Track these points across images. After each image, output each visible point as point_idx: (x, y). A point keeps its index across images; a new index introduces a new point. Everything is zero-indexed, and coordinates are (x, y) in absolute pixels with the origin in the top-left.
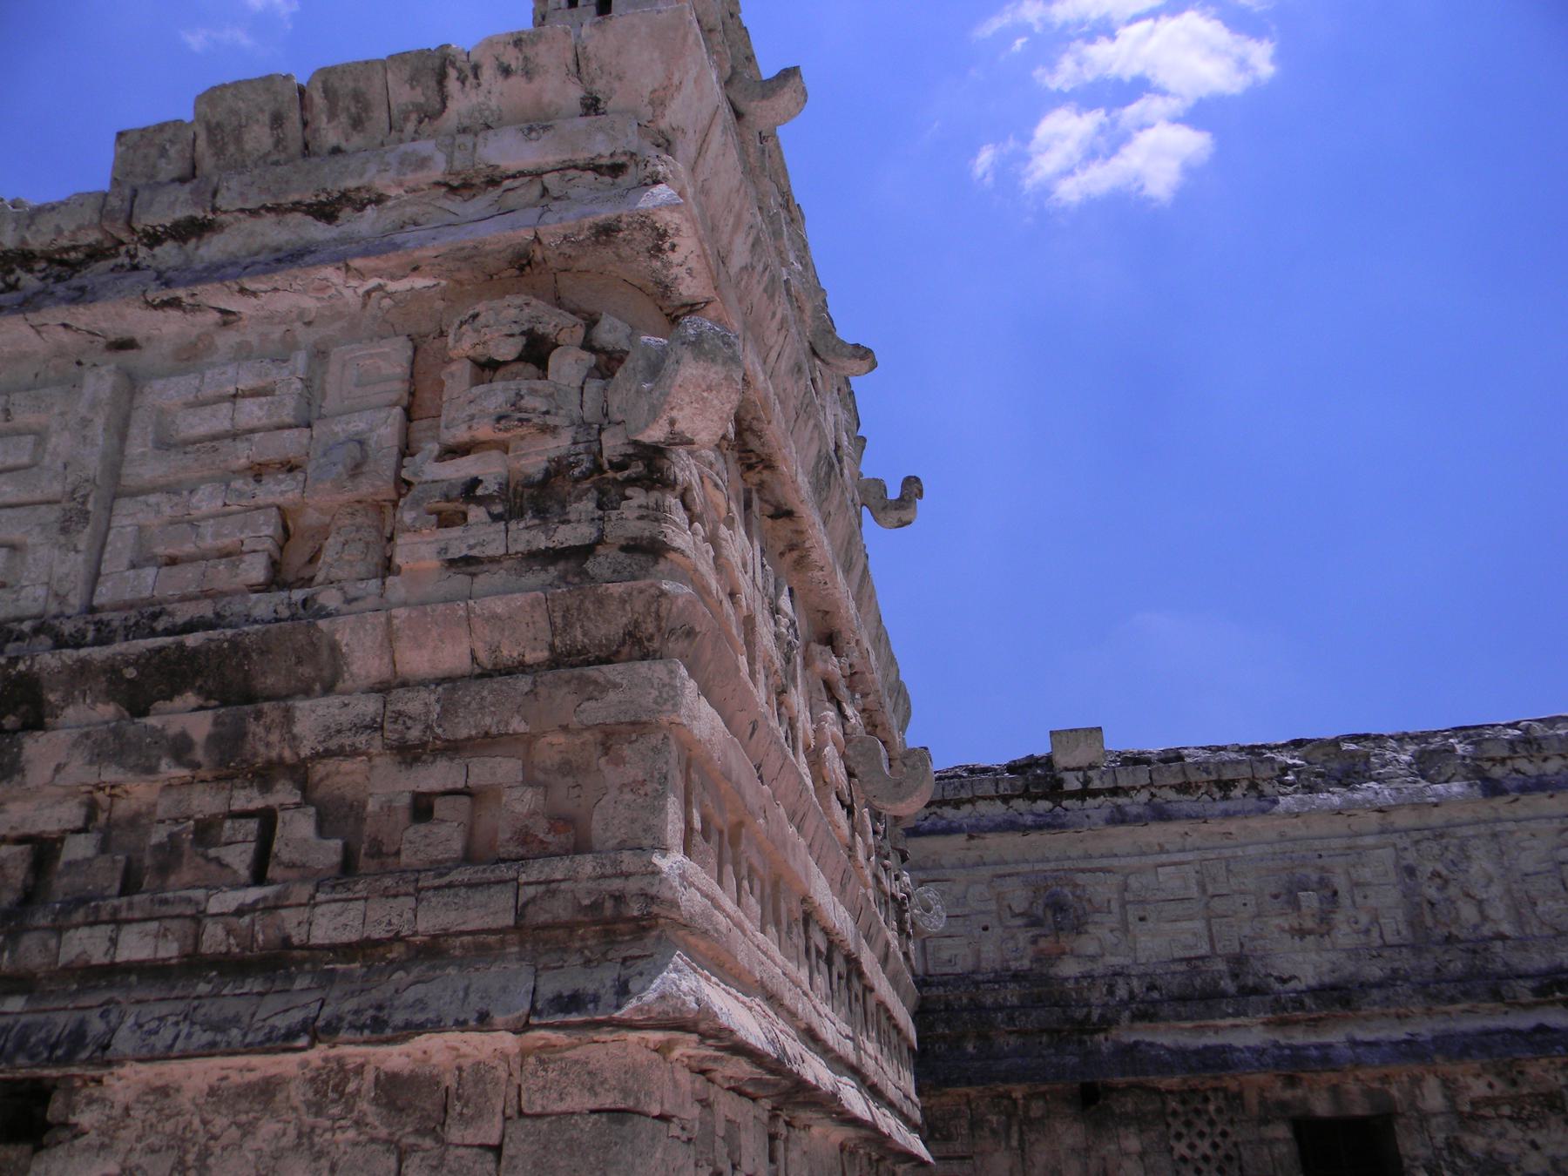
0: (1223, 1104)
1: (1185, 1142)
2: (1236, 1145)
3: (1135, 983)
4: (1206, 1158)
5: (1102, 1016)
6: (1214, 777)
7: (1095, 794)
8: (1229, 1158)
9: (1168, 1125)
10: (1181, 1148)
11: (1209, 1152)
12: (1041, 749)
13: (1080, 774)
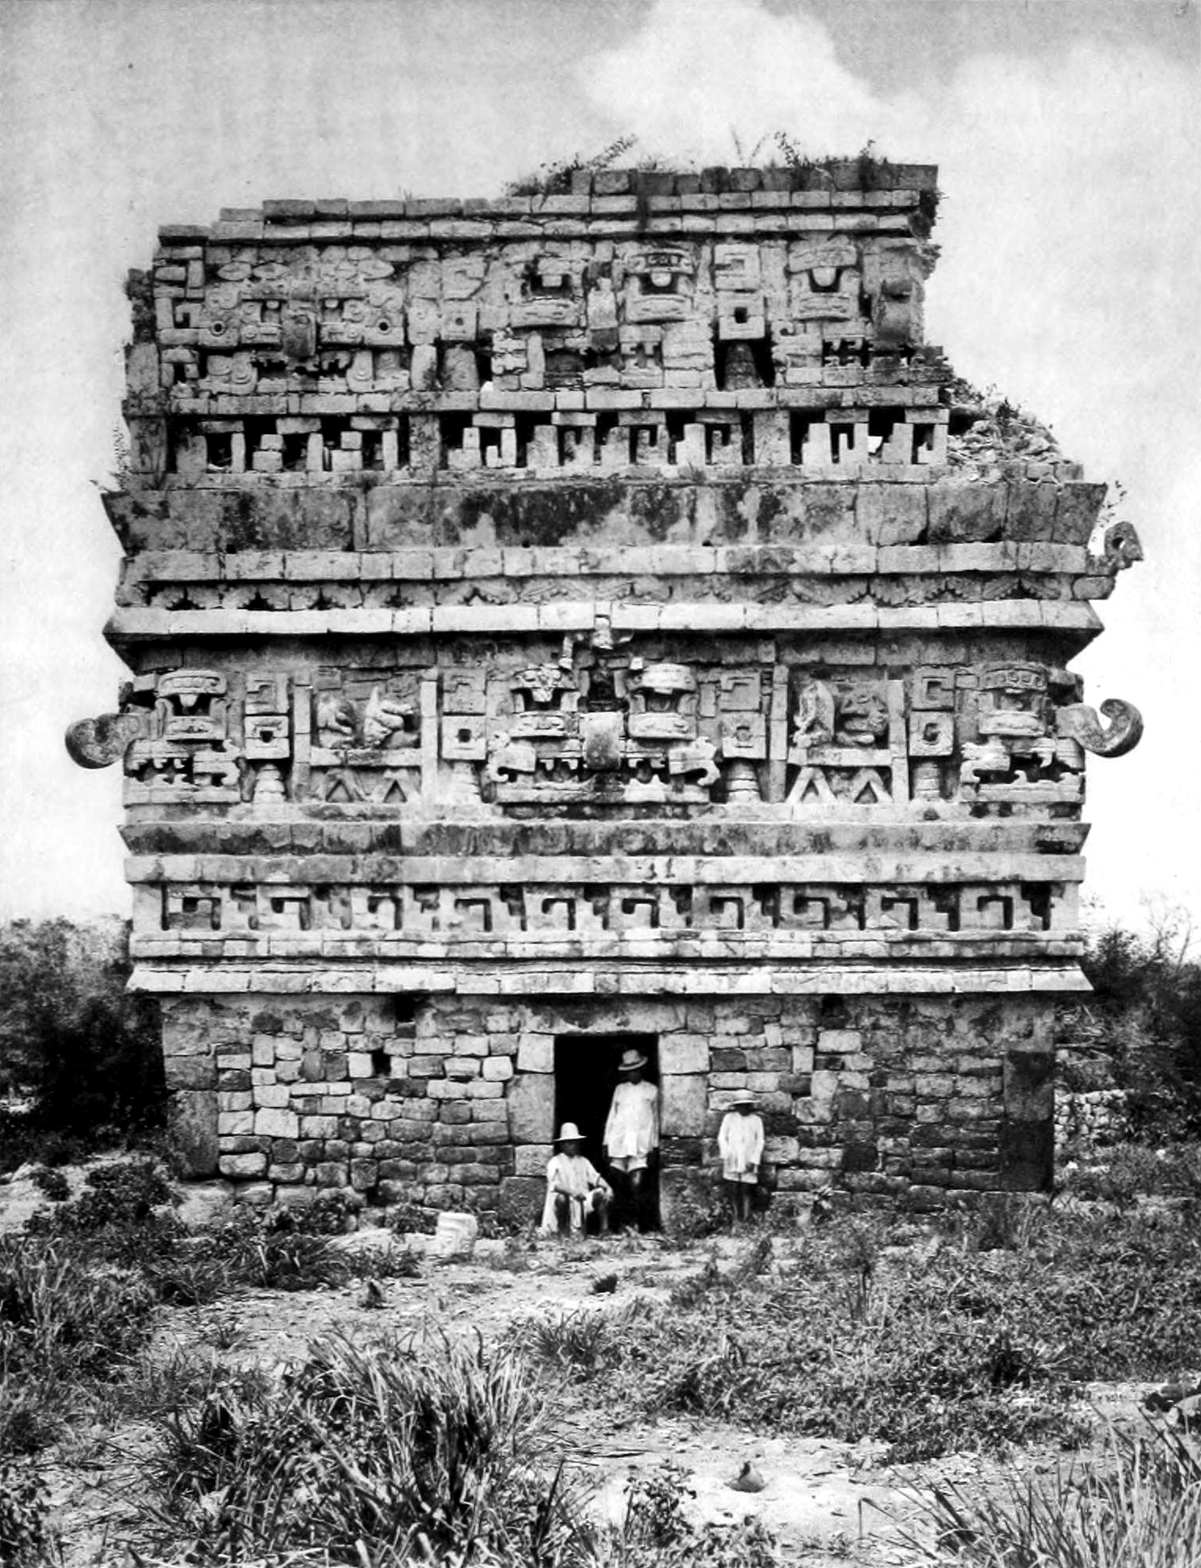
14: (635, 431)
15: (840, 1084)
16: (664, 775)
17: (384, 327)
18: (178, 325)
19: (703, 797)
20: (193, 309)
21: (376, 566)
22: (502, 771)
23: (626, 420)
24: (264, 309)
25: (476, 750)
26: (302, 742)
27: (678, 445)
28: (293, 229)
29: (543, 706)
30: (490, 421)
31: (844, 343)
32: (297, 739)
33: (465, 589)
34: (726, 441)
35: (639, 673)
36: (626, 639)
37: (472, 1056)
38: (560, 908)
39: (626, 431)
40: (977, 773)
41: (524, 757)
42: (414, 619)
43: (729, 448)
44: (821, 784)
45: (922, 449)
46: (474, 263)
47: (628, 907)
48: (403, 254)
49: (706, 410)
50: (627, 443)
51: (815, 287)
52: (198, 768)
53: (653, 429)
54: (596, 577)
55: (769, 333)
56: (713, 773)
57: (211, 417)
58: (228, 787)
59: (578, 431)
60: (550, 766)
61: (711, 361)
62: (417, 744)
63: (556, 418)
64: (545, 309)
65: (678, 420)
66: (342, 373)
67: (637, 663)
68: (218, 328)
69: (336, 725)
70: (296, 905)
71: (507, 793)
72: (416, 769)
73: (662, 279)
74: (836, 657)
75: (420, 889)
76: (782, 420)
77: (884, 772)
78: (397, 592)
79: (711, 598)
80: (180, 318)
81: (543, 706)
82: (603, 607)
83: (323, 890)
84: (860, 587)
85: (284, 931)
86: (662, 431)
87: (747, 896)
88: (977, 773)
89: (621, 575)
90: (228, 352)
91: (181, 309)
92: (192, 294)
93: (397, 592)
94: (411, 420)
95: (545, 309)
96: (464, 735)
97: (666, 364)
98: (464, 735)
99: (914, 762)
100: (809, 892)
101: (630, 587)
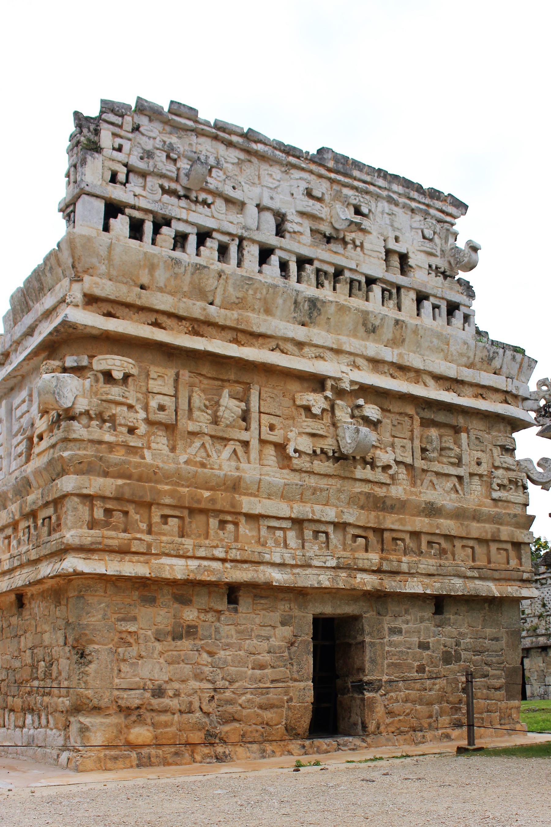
14: (352, 281)
16: (373, 465)
22: (296, 451)
23: (347, 274)
25: (277, 437)
27: (370, 293)
29: (314, 416)
30: (285, 256)
33: (273, 344)
34: (390, 298)
35: (359, 407)
36: (356, 387)
39: (348, 280)
43: (391, 302)
50: (348, 286)
54: (338, 352)
55: (408, 253)
56: (395, 467)
58: (139, 437)
59: (326, 273)
60: (318, 451)
61: (384, 257)
62: (246, 429)
63: (317, 264)
65: (371, 281)
67: (361, 402)
69: (204, 408)
70: (176, 520)
72: (246, 444)
74: (441, 417)
76: (413, 295)
77: (460, 478)
78: (242, 335)
79: (388, 374)
81: (314, 416)
83: (192, 511)
87: (407, 537)
89: (350, 354)
96: (272, 428)
97: (366, 251)
98: (272, 428)
99: (472, 475)
101: (355, 359)
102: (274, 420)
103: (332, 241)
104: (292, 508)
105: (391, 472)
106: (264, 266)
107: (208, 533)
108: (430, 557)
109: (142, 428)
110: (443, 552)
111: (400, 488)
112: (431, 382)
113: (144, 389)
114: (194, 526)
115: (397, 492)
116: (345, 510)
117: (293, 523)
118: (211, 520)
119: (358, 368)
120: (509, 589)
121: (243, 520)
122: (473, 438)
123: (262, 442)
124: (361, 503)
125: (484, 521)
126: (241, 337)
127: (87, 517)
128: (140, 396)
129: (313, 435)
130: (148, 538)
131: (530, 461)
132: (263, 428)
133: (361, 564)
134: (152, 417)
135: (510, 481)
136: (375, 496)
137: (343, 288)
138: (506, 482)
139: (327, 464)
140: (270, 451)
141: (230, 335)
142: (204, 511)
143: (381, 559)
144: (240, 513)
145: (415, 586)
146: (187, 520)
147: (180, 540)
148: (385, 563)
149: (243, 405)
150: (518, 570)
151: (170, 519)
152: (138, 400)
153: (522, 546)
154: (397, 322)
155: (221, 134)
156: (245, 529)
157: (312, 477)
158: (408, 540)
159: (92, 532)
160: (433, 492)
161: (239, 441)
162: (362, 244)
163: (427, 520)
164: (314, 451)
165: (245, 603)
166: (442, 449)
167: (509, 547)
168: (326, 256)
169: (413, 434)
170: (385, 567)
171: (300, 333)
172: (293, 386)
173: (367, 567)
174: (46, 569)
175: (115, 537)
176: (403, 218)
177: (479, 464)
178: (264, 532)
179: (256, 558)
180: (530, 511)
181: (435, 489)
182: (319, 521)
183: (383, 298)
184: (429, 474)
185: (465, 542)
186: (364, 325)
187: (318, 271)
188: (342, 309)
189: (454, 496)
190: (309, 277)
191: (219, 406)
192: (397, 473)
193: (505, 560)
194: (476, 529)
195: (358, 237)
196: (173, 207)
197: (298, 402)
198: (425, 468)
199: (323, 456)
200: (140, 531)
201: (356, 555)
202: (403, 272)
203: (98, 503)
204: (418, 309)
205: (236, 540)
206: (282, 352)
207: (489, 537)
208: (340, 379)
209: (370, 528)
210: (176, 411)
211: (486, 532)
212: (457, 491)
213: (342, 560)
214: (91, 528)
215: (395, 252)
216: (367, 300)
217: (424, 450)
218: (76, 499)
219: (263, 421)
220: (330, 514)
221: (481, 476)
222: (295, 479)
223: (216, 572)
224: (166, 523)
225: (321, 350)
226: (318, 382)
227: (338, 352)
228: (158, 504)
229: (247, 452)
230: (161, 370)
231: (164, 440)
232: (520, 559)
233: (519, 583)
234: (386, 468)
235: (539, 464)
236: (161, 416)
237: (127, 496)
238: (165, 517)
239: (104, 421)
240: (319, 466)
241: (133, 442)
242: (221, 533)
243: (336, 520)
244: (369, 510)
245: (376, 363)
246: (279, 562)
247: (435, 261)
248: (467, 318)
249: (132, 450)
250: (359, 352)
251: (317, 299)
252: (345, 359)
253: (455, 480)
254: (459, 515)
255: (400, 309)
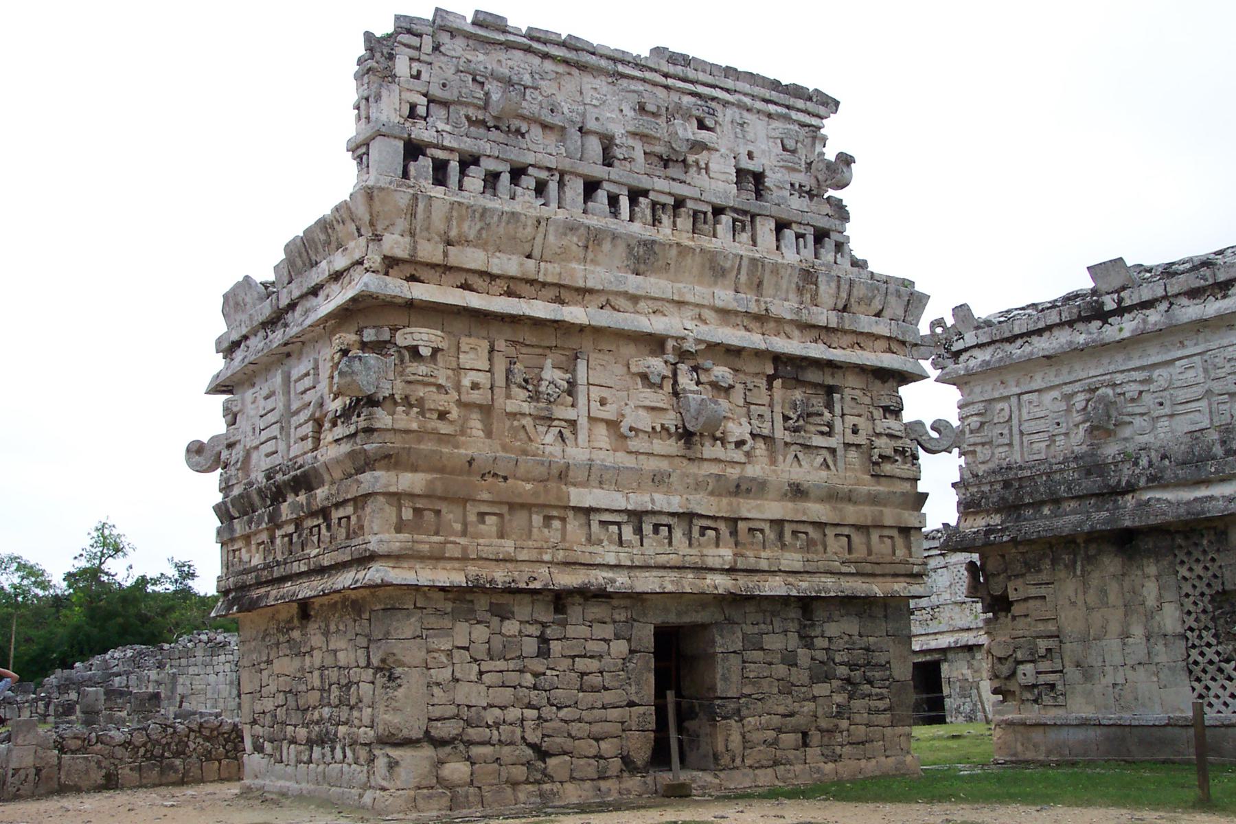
0: (1213, 538)
1: (1186, 566)
2: (1220, 567)
3: (1153, 454)
4: (1200, 577)
5: (1128, 482)
6: (1211, 281)
7: (1129, 309)
8: (1215, 576)
9: (1175, 556)
10: (1183, 571)
11: (1201, 574)
12: (1087, 284)
13: (1115, 296)
14: (695, 213)
15: (813, 659)
16: (724, 442)
17: (552, 111)
18: (412, 76)
19: (743, 460)
20: (425, 69)
21: (550, 272)
22: (631, 429)
24: (474, 80)
25: (609, 412)
26: (500, 393)
28: (489, 31)
31: (800, 186)
32: (496, 390)
33: (603, 300)
34: (743, 229)
36: (703, 347)
37: (604, 640)
38: (664, 531)
39: (691, 212)
40: (880, 456)
41: (645, 421)
42: (575, 314)
43: (744, 235)
44: (800, 455)
45: (839, 256)
46: (601, 83)
47: (703, 530)
48: (561, 69)
49: (735, 210)
51: (784, 149)
52: (429, 405)
53: (705, 213)
54: (680, 304)
56: (750, 442)
57: (436, 146)
58: (451, 422)
59: (664, 206)
60: (658, 429)
63: (652, 195)
64: (646, 125)
65: (718, 211)
66: (523, 135)
68: (444, 85)
70: (494, 518)
71: (634, 444)
72: (573, 423)
73: (709, 122)
75: (577, 510)
76: (773, 226)
77: (833, 451)
80: (415, 73)
81: (651, 385)
82: (689, 325)
83: (512, 507)
84: (815, 333)
85: (487, 539)
86: (710, 215)
87: (766, 527)
88: (880, 456)
90: (445, 104)
91: (416, 66)
92: (423, 57)
93: (562, 292)
94: (567, 178)
95: (646, 125)
96: (603, 402)
98: (603, 402)
99: (847, 445)
100: (801, 528)
102: (605, 393)
103: (671, 164)
104: (628, 498)
105: (746, 448)
106: (590, 204)
107: (530, 531)
108: (793, 548)
109: (455, 413)
110: (810, 544)
111: (758, 467)
112: (797, 333)
113: (454, 365)
114: (515, 524)
115: (753, 471)
116: (691, 497)
117: (629, 516)
118: (534, 517)
119: (705, 322)
120: (896, 587)
121: (571, 514)
122: (848, 398)
123: (591, 419)
124: (710, 488)
125: (863, 503)
126: (565, 295)
127: (394, 519)
128: (450, 372)
129: (653, 409)
130: (463, 541)
131: (920, 423)
132: (592, 403)
133: (710, 562)
134: (464, 398)
135: (896, 451)
136: (727, 479)
137: (684, 222)
138: (890, 452)
139: (668, 442)
140: (602, 430)
141: (552, 293)
142: (527, 507)
143: (735, 555)
144: (566, 507)
145: (774, 586)
146: (507, 517)
147: (499, 541)
148: (739, 560)
149: (568, 376)
150: (907, 563)
151: (487, 518)
152: (448, 378)
153: (912, 532)
154: (753, 261)
155: (535, 45)
156: (574, 526)
157: (652, 459)
158: (767, 531)
159: (401, 536)
160: (798, 469)
161: (566, 421)
162: (707, 164)
163: (790, 505)
164: (653, 428)
165: (575, 613)
166: (809, 415)
167: (895, 533)
168: (661, 186)
169: (772, 399)
170: (739, 566)
171: (633, 283)
172: (628, 350)
173: (718, 566)
174: (345, 579)
175: (427, 542)
176: (758, 127)
177: (855, 431)
178: (595, 527)
179: (586, 559)
180: (922, 487)
181: (800, 465)
182: (660, 513)
183: (734, 231)
184: (793, 447)
185: (839, 530)
186: (712, 268)
187: (654, 204)
188: (683, 250)
189: (824, 473)
190: (643, 213)
191: (541, 379)
192: (753, 448)
193: (890, 551)
194: (852, 513)
195: (703, 157)
196: (483, 146)
197: (634, 369)
198: (788, 440)
199: (664, 433)
200: (456, 534)
201: (705, 552)
202: (759, 194)
203: (406, 502)
204: (778, 240)
205: (564, 539)
206: (614, 308)
207: (869, 523)
208: (683, 338)
209: (722, 518)
210: (492, 388)
211: (866, 516)
212: (828, 467)
213: (688, 558)
214: (398, 530)
215: (748, 172)
216: (715, 236)
217: (786, 418)
218: (381, 499)
219: (592, 395)
220: (675, 503)
221: (858, 446)
222: (630, 461)
223: (543, 577)
224: (483, 522)
225: (660, 303)
226: (656, 343)
227: (680, 304)
228: (474, 500)
229: (574, 433)
230: (472, 340)
231: (479, 425)
232: (909, 548)
233: (908, 580)
234: (740, 444)
235: (933, 428)
236: (476, 397)
237: (439, 492)
238: (482, 516)
239: (411, 406)
240: (659, 446)
241: (444, 428)
242: (546, 531)
243: (681, 511)
244: (720, 495)
245: (725, 314)
246: (612, 562)
247: (800, 178)
248: (840, 247)
249: (442, 438)
250: (706, 302)
251: (654, 242)
252: (689, 312)
253: (825, 452)
254: (833, 496)
255: (755, 244)
